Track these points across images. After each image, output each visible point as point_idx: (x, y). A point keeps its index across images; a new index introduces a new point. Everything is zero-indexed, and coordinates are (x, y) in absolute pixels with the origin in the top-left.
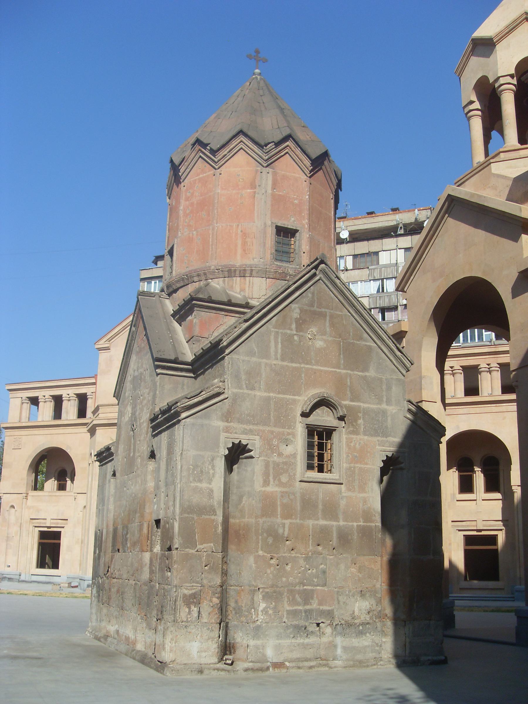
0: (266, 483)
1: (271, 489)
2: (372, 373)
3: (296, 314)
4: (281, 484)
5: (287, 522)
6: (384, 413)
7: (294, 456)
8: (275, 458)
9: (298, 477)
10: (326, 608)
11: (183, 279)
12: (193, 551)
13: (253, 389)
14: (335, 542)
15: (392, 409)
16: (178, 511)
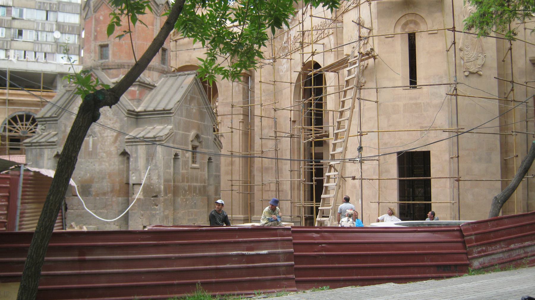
0: (183, 169)
1: (184, 171)
2: (206, 123)
3: (189, 98)
4: (186, 169)
5: (187, 184)
6: (208, 139)
7: (188, 158)
8: (184, 159)
9: (190, 166)
10: (196, 217)
11: (118, 65)
12: (166, 197)
13: (179, 130)
14: (197, 192)
15: (210, 137)
16: (162, 181)
